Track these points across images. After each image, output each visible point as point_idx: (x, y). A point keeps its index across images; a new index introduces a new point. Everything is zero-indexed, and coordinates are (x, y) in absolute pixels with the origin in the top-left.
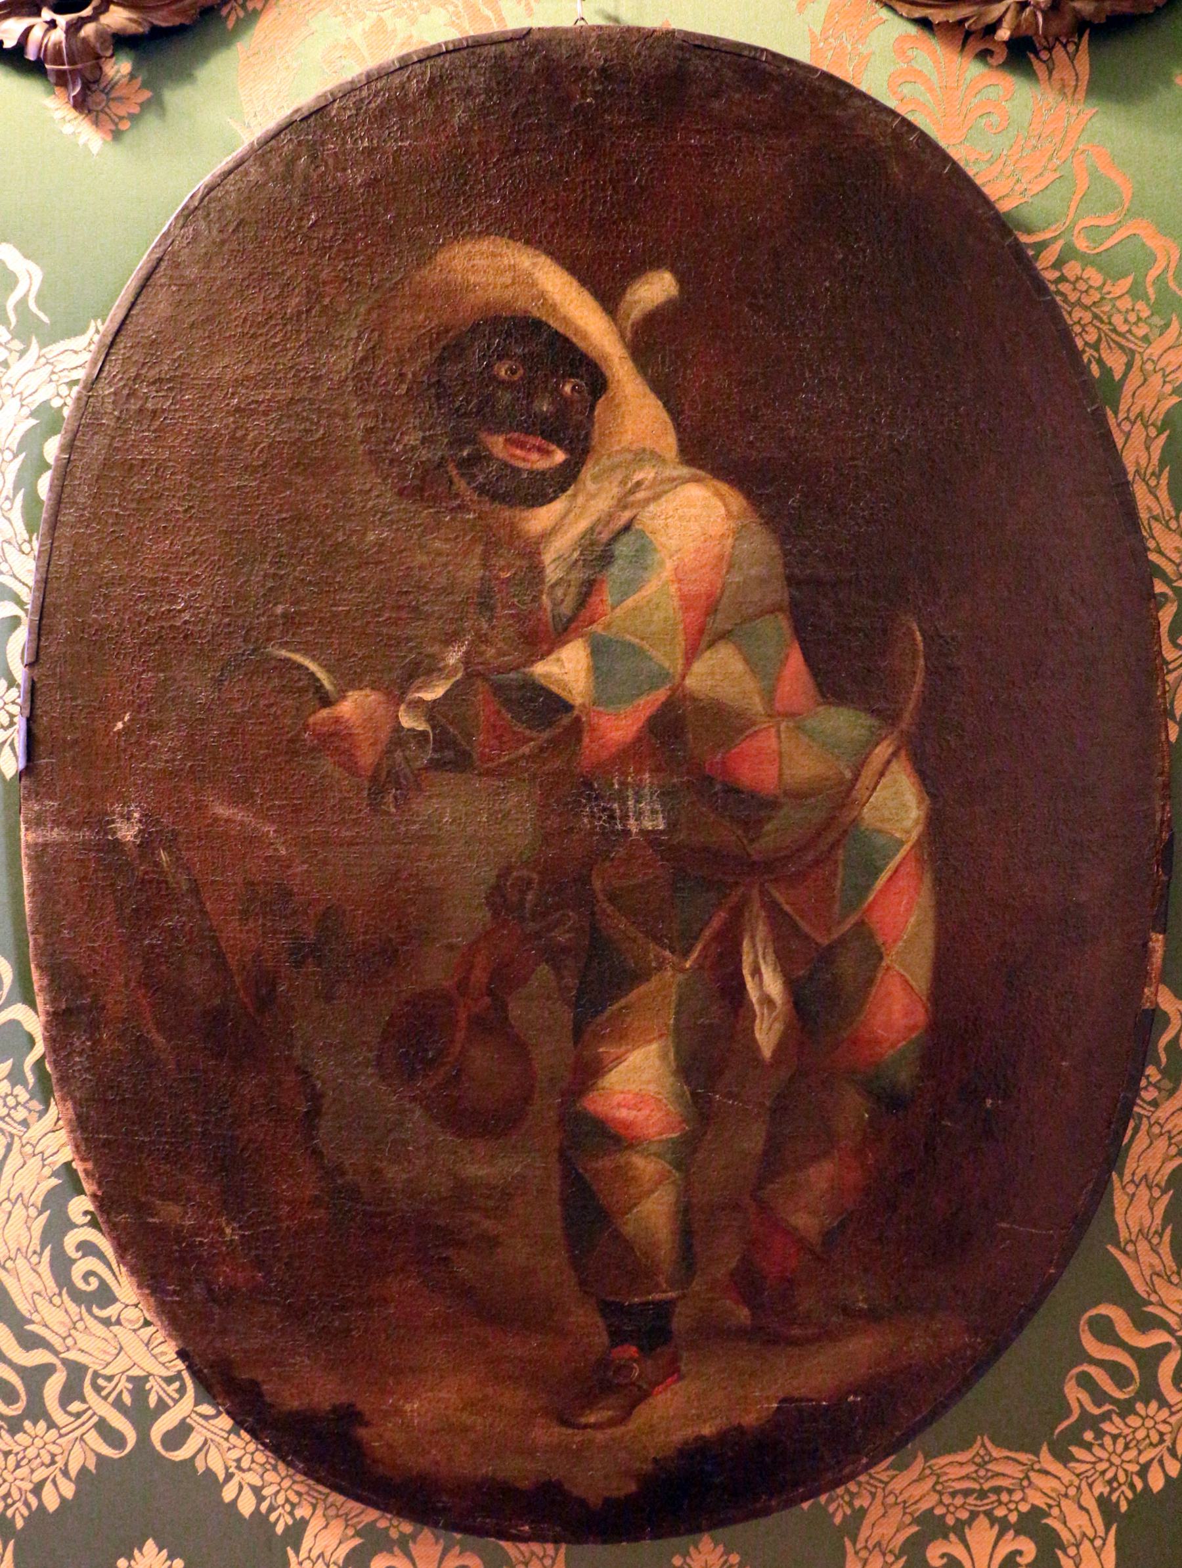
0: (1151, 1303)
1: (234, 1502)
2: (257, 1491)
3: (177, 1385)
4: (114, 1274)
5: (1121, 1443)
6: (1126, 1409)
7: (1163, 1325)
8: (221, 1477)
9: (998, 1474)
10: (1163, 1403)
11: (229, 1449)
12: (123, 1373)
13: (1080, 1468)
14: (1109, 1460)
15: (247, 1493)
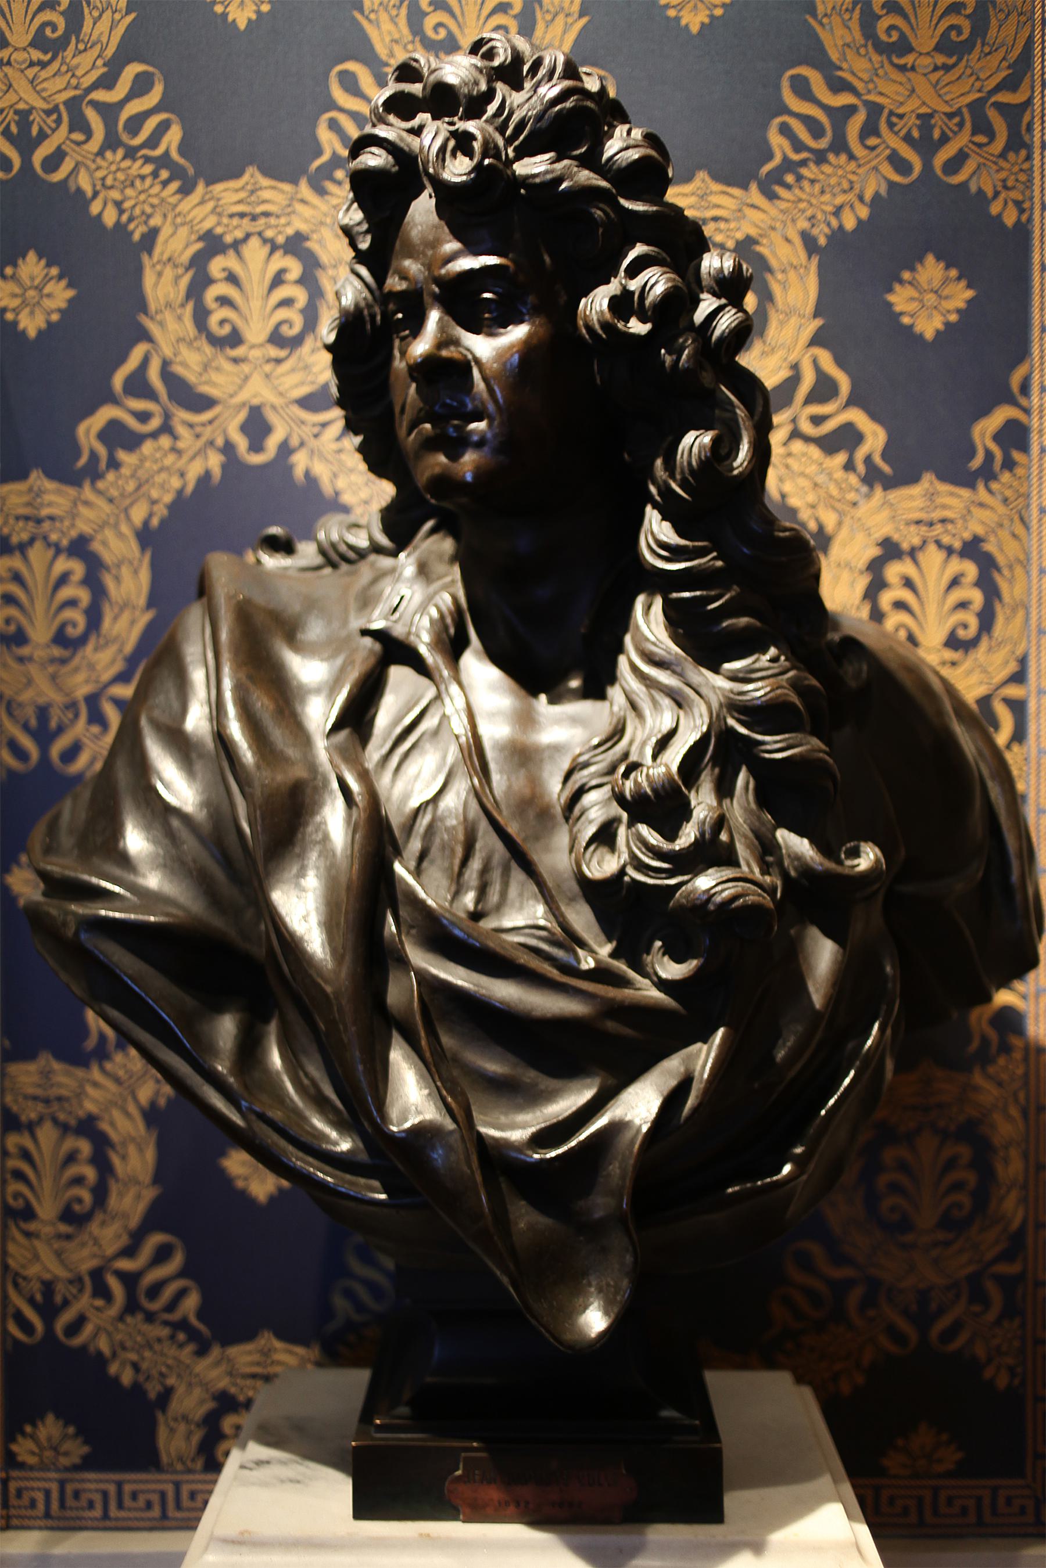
2: (118, 204)
3: (54, 116)
4: (8, 23)
5: (817, 187)
6: (820, 157)
8: (89, 193)
9: (718, 206)
10: (852, 157)
12: (11, 106)
13: (783, 205)
14: (809, 202)
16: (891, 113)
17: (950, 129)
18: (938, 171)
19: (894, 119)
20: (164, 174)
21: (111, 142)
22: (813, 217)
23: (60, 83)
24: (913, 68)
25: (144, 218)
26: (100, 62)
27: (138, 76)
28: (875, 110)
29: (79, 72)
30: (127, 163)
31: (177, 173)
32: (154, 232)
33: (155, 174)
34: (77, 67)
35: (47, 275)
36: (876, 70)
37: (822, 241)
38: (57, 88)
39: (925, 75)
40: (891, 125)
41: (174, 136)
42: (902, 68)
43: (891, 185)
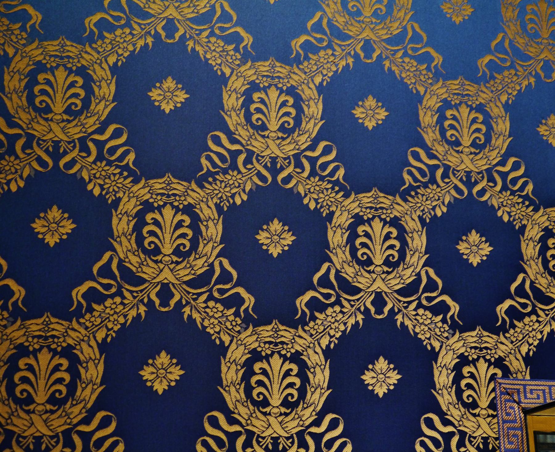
25: (327, 207)
27: (326, 146)
29: (300, 143)
34: (299, 141)
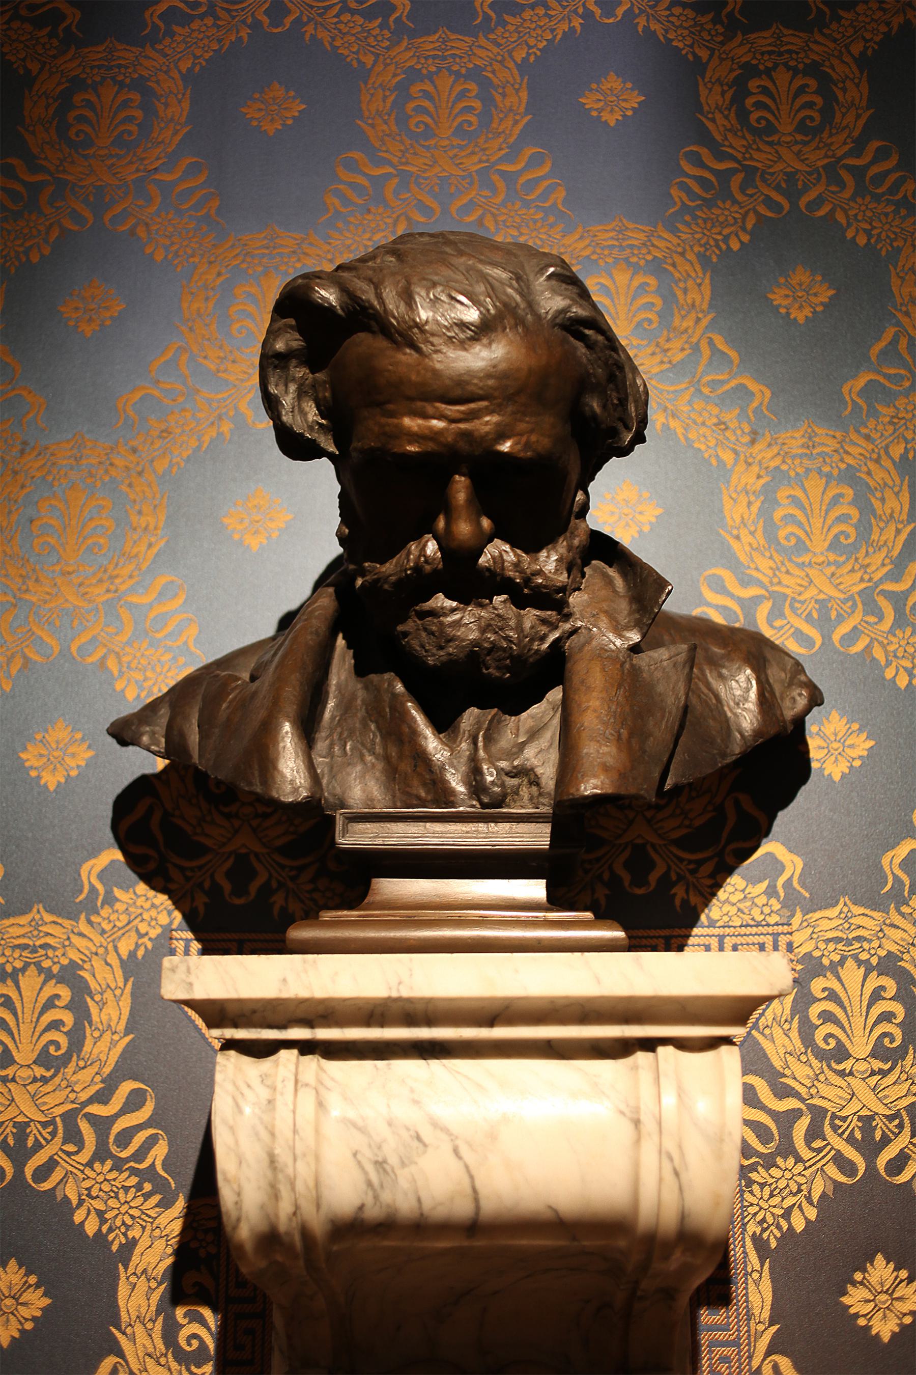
0: (785, 1076)
1: (83, 1223)
2: (100, 1214)
5: (767, 1191)
6: (769, 1162)
7: (797, 1095)
8: (75, 1202)
10: (799, 1159)
11: (84, 1179)
15: (93, 1214)
16: (834, 1116)
17: (890, 1130)
18: (882, 1172)
19: (837, 1122)
20: (148, 1187)
21: (102, 1154)
22: (764, 1220)
23: (61, 1096)
24: (851, 1073)
26: (98, 1078)
28: (818, 1113)
30: (114, 1174)
31: (160, 1186)
32: (132, 1243)
33: (139, 1187)
35: (26, 1282)
36: (817, 1075)
37: (773, 1244)
38: (56, 1102)
39: (864, 1079)
40: (835, 1128)
41: (160, 1151)
42: (842, 1074)
43: (837, 1185)
